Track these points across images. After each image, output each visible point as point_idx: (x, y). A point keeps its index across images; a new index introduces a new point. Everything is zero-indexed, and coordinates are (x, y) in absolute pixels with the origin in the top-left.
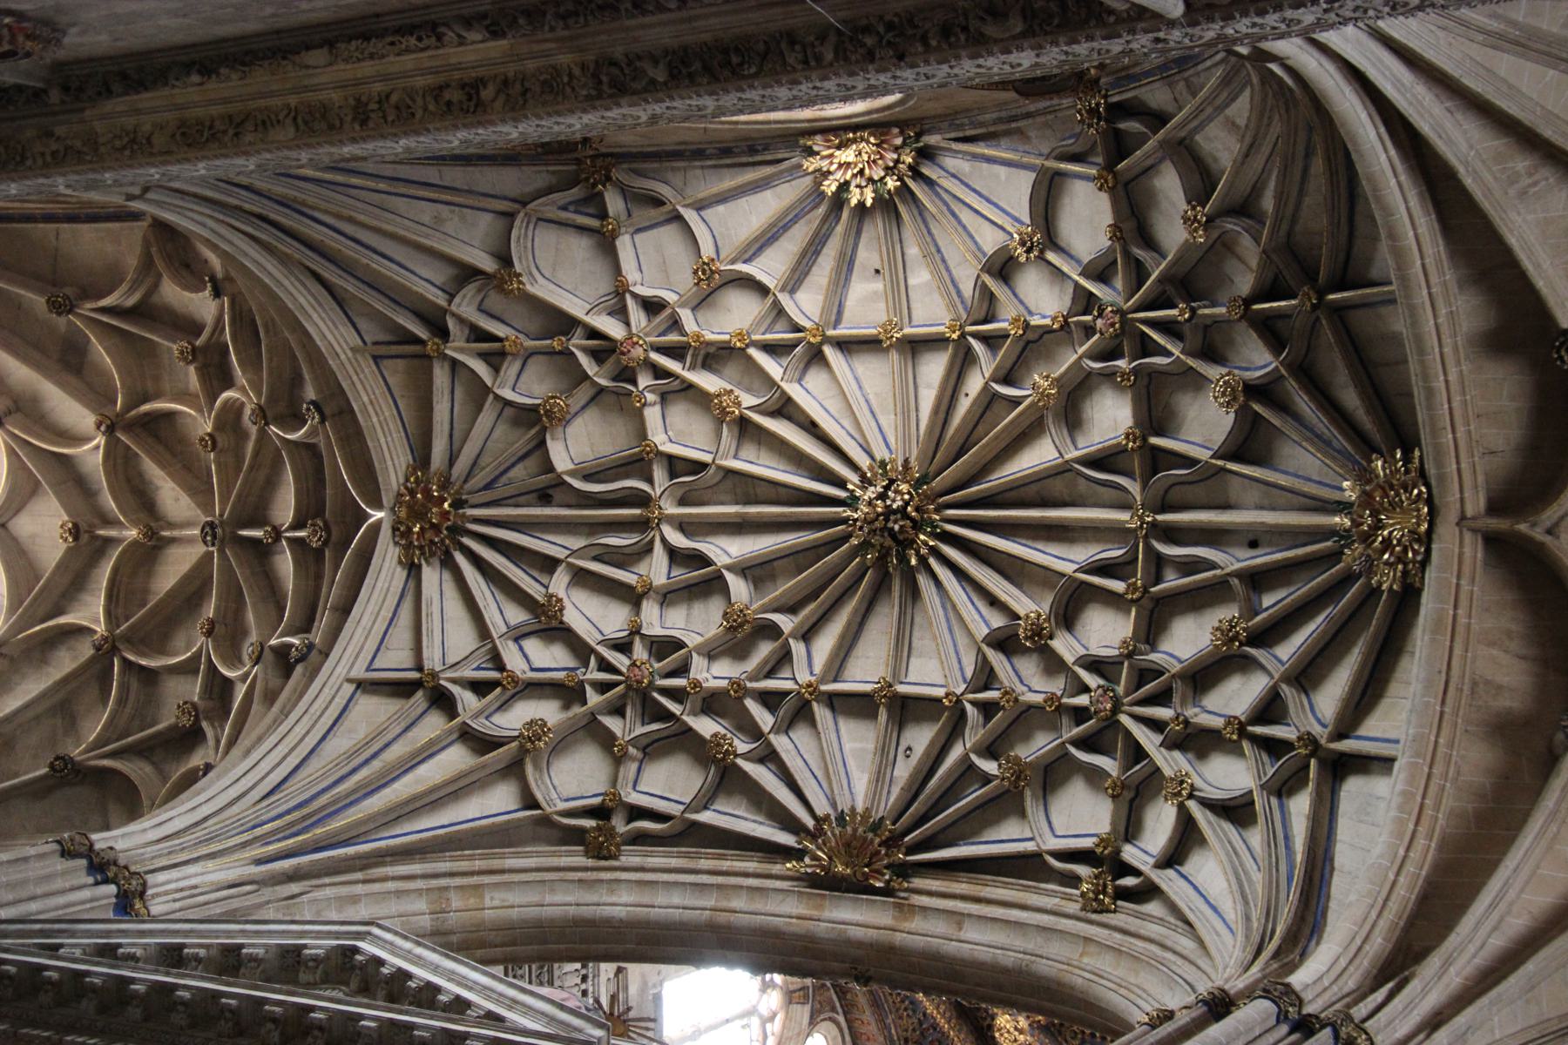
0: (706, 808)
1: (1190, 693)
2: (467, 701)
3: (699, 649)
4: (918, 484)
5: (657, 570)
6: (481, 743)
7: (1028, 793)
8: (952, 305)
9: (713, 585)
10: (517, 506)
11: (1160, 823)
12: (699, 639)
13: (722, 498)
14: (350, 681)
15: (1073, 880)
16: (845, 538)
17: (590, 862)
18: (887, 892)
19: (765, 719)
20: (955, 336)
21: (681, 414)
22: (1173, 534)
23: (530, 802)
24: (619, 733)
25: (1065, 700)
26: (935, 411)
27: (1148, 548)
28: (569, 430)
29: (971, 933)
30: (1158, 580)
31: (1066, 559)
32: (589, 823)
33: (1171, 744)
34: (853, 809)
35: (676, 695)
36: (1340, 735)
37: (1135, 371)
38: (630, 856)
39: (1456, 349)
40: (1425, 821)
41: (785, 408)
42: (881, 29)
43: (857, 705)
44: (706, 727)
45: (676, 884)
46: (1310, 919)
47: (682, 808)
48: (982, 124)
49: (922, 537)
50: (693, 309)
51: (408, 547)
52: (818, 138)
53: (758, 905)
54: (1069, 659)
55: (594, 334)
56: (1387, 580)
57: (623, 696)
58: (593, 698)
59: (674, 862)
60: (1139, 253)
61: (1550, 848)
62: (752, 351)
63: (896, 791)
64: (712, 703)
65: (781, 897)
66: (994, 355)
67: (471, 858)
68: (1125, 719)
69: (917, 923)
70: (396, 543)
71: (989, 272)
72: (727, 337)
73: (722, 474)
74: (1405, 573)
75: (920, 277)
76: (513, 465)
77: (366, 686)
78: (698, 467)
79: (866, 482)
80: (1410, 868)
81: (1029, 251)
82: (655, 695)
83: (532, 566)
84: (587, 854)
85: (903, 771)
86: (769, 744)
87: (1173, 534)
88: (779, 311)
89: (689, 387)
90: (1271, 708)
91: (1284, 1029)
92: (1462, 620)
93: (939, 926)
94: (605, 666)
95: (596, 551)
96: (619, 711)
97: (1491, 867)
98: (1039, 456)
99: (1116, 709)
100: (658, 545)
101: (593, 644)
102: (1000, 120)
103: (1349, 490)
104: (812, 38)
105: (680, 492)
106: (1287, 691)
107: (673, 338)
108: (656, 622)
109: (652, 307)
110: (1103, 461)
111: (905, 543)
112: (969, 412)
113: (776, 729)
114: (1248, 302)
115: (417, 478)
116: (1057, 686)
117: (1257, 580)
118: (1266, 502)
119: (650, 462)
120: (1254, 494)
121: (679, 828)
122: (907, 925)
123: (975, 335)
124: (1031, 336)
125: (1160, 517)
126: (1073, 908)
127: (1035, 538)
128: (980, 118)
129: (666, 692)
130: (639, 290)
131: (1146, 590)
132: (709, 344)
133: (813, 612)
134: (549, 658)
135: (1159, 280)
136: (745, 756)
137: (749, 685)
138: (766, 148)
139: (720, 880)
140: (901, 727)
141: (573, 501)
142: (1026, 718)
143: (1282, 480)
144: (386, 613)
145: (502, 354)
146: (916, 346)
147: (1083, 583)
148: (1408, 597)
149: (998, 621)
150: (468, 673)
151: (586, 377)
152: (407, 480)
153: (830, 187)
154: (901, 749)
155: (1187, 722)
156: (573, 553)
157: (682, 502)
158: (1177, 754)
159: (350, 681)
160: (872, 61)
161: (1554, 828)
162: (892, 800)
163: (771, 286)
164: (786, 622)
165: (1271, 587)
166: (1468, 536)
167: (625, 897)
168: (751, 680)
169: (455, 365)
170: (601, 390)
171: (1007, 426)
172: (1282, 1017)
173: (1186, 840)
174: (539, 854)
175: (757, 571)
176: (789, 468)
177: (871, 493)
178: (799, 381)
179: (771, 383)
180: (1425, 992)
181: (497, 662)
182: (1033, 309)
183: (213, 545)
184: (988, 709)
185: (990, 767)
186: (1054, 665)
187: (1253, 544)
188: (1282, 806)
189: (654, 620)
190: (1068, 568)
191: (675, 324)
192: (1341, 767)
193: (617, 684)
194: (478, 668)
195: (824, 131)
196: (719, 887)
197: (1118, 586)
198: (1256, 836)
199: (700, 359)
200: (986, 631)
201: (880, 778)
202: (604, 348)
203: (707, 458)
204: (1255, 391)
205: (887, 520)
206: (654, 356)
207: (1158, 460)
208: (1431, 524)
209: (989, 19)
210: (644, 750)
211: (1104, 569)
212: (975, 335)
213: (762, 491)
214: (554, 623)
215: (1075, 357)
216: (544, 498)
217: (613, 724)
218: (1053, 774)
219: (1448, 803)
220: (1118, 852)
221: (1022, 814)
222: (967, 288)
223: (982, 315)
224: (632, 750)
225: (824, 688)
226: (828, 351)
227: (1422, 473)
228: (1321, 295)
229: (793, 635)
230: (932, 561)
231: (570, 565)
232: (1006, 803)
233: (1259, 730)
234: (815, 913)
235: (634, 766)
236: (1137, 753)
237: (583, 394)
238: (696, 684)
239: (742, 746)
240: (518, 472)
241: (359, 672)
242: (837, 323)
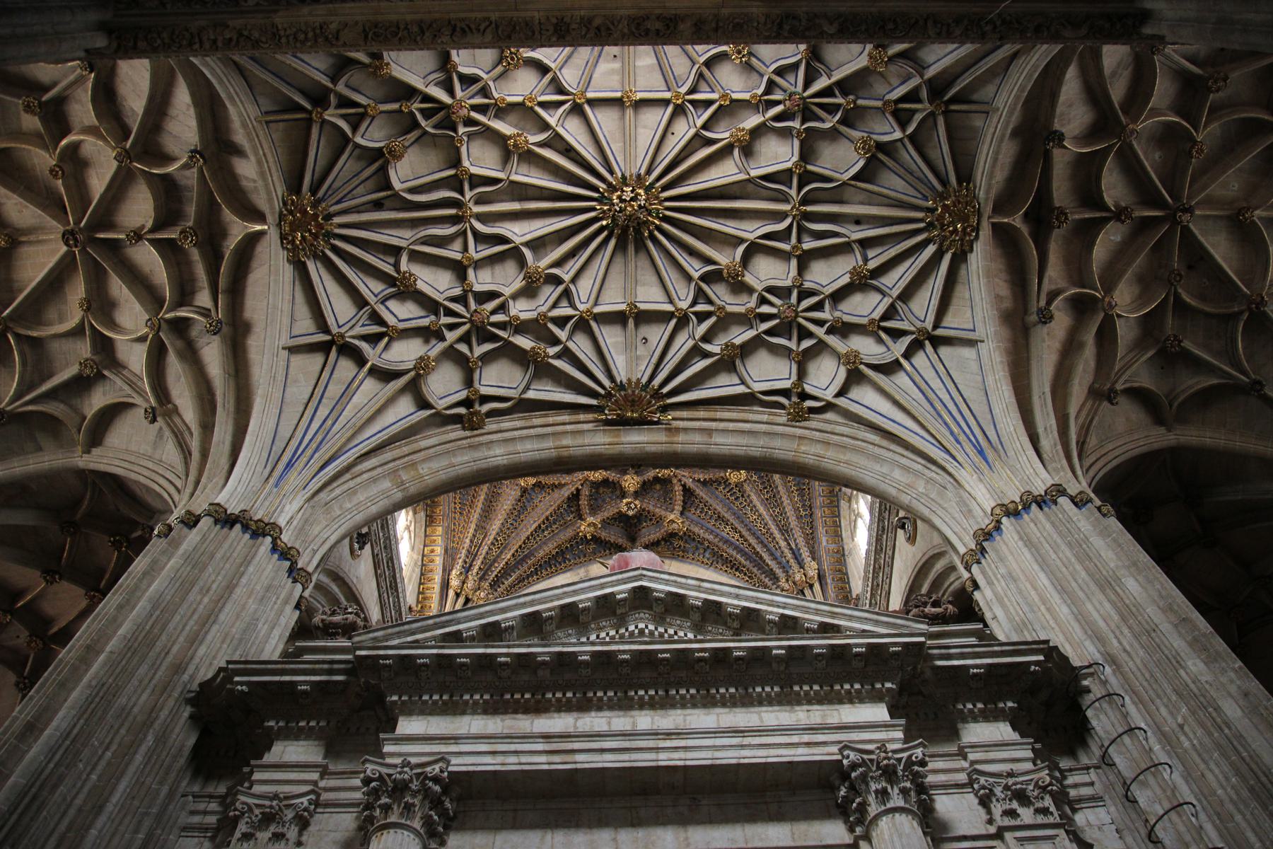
2: (364, 346)
4: (648, 189)
6: (384, 375)
9: (515, 254)
10: (358, 212)
13: (504, 197)
14: (283, 348)
15: (780, 406)
17: (468, 433)
19: (562, 335)
23: (423, 404)
29: (718, 439)
32: (462, 410)
33: (828, 332)
35: (502, 326)
38: (491, 425)
44: (525, 342)
45: (527, 437)
50: (494, 81)
51: (295, 249)
53: (579, 441)
55: (427, 98)
57: (468, 333)
59: (518, 424)
65: (592, 433)
67: (400, 447)
68: (800, 320)
69: (681, 438)
70: (283, 248)
77: (293, 350)
83: (378, 252)
84: (464, 429)
90: (890, 313)
93: (697, 438)
99: (797, 316)
101: (441, 301)
104: (950, 21)
106: (899, 305)
115: (293, 200)
117: (865, 244)
122: (675, 439)
126: (784, 419)
129: (494, 325)
130: (460, 69)
134: (402, 312)
136: (552, 357)
139: (549, 430)
142: (726, 320)
143: (885, 191)
144: (288, 297)
145: (362, 117)
150: (359, 330)
151: (416, 125)
152: (285, 204)
154: (639, 339)
157: (477, 203)
158: (832, 336)
159: (283, 348)
163: (553, 66)
167: (498, 450)
169: (324, 122)
174: (436, 435)
175: (538, 245)
176: (550, 178)
181: (376, 318)
183: (76, 246)
186: (740, 288)
187: (858, 222)
191: (485, 92)
194: (363, 325)
196: (554, 434)
201: (634, 360)
202: (435, 109)
203: (501, 175)
204: (881, 146)
213: (531, 193)
216: (378, 205)
217: (463, 348)
218: (747, 350)
233: (883, 324)
234: (616, 440)
241: (285, 341)
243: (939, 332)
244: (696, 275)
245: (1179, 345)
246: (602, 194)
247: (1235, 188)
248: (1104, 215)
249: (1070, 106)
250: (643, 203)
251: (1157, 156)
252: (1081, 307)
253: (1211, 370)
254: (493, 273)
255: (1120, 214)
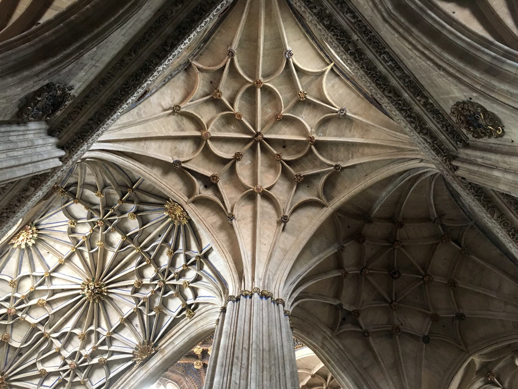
0: (110, 374)
1: (173, 268)
3: (81, 349)
4: (93, 281)
5: (58, 344)
7: (164, 311)
8: (68, 246)
9: (72, 336)
11: (188, 293)
12: (78, 348)
13: (57, 319)
15: (184, 316)
16: (89, 302)
18: (156, 352)
19: (105, 348)
20: (75, 250)
21: (34, 313)
22: (146, 247)
24: (79, 380)
25: (154, 290)
26: (84, 266)
27: (144, 252)
28: (13, 338)
29: (176, 343)
30: (151, 256)
31: (132, 267)
33: (178, 279)
34: (137, 345)
35: (84, 361)
36: (201, 251)
37: (113, 227)
39: (160, 179)
40: (225, 252)
41: (54, 292)
42: (5, 211)
43: (120, 327)
44: (95, 361)
46: (223, 283)
47: (105, 379)
48: (43, 211)
49: (103, 289)
50: (17, 292)
52: (12, 240)
53: (136, 379)
54: (149, 283)
56: (185, 222)
57: (74, 372)
58: (68, 379)
60: (94, 208)
61: (243, 239)
62: (37, 289)
63: (141, 334)
64: (92, 356)
65: (139, 373)
66: (85, 247)
68: (167, 283)
69: (166, 351)
71: (70, 234)
72: (29, 291)
73: (53, 316)
74: (186, 218)
75: (57, 246)
76: (7, 356)
78: (47, 318)
79: (83, 290)
80: (229, 261)
81: (74, 224)
82: (80, 366)
83: (31, 369)
85: (139, 330)
86: (111, 351)
87: (146, 247)
88: (36, 277)
89: (30, 307)
91: (236, 303)
92: (201, 218)
93: (170, 347)
94: (64, 371)
95: (41, 353)
96: (76, 376)
97: (239, 249)
98: (110, 256)
99: (164, 282)
100: (53, 340)
102: (46, 207)
103: (166, 214)
105: (48, 327)
106: (187, 253)
107: (18, 301)
108: (67, 353)
109: (7, 300)
110: (122, 246)
111: (101, 293)
112: (90, 260)
113: (109, 347)
114: (121, 199)
116: (151, 289)
117: (166, 241)
118: (155, 228)
119: (36, 327)
120: (152, 228)
121: (108, 383)
123: (78, 247)
124: (89, 238)
125: (141, 246)
126: (188, 320)
127: (123, 269)
128: (42, 210)
129: (82, 363)
131: (150, 259)
132: (26, 296)
133: (96, 321)
135: (103, 209)
136: (108, 358)
137: (96, 345)
138: (3, 251)
140: (131, 323)
141: (27, 349)
142: (151, 299)
143: (154, 222)
146: (69, 259)
147: (139, 268)
148: (190, 221)
149: (130, 289)
153: (23, 246)
155: (177, 273)
156: (37, 358)
157: (50, 328)
158: (180, 280)
160: (9, 218)
161: (241, 235)
162: (142, 336)
164: (92, 328)
165: (169, 240)
166: (190, 205)
168: (96, 344)
170: (12, 324)
171: (100, 257)
172: (234, 302)
173: (195, 291)
175: (78, 325)
176: (65, 301)
177: (86, 290)
178: (52, 285)
179: (47, 290)
180: (248, 276)
182: (84, 233)
184: (143, 304)
185: (153, 313)
186: (147, 286)
187: (160, 236)
188: (204, 271)
189: (66, 353)
190: (134, 269)
191: (16, 298)
192: (206, 256)
193: (71, 371)
195: (12, 238)
196: (126, 384)
197: (145, 263)
198: (204, 279)
199: (28, 300)
200: (130, 293)
201: (136, 335)
203: (47, 315)
204: (135, 213)
205: (94, 292)
206: (17, 308)
207: (131, 238)
208: (183, 208)
209: (26, 192)
210: (88, 377)
211: (140, 263)
212: (78, 247)
213: (64, 310)
214: (46, 375)
215: (100, 234)
216: (20, 355)
217: (77, 379)
218: (164, 304)
219: (225, 246)
220: (186, 304)
221: (166, 315)
222: (69, 240)
223: (76, 242)
224: (85, 380)
225: (111, 331)
226: (52, 275)
227: (174, 201)
228: (131, 188)
229: (96, 328)
230: (109, 291)
231: (38, 361)
232: (161, 316)
233: (189, 263)
235: (89, 382)
236: (174, 286)
237: (9, 329)
238: (86, 356)
239: (106, 357)
240: (10, 356)
242: (49, 268)
243: (203, 252)
244: (129, 293)
245: (301, 177)
246: (82, 294)
247: (270, 111)
248: (231, 162)
249: (176, 148)
250: (93, 287)
251: (232, 127)
252: (251, 197)
253: (324, 173)
254: (72, 346)
255: (238, 157)
